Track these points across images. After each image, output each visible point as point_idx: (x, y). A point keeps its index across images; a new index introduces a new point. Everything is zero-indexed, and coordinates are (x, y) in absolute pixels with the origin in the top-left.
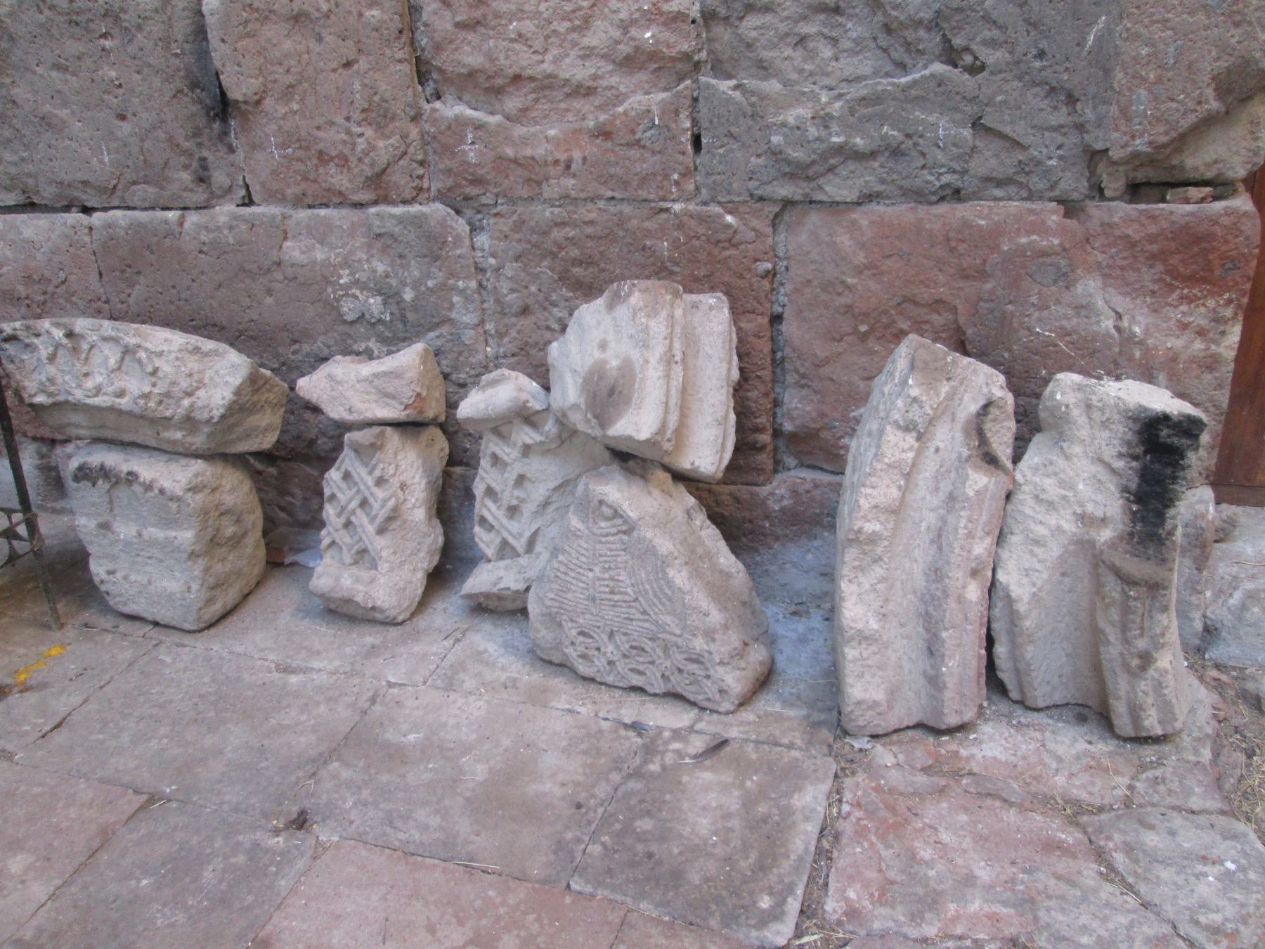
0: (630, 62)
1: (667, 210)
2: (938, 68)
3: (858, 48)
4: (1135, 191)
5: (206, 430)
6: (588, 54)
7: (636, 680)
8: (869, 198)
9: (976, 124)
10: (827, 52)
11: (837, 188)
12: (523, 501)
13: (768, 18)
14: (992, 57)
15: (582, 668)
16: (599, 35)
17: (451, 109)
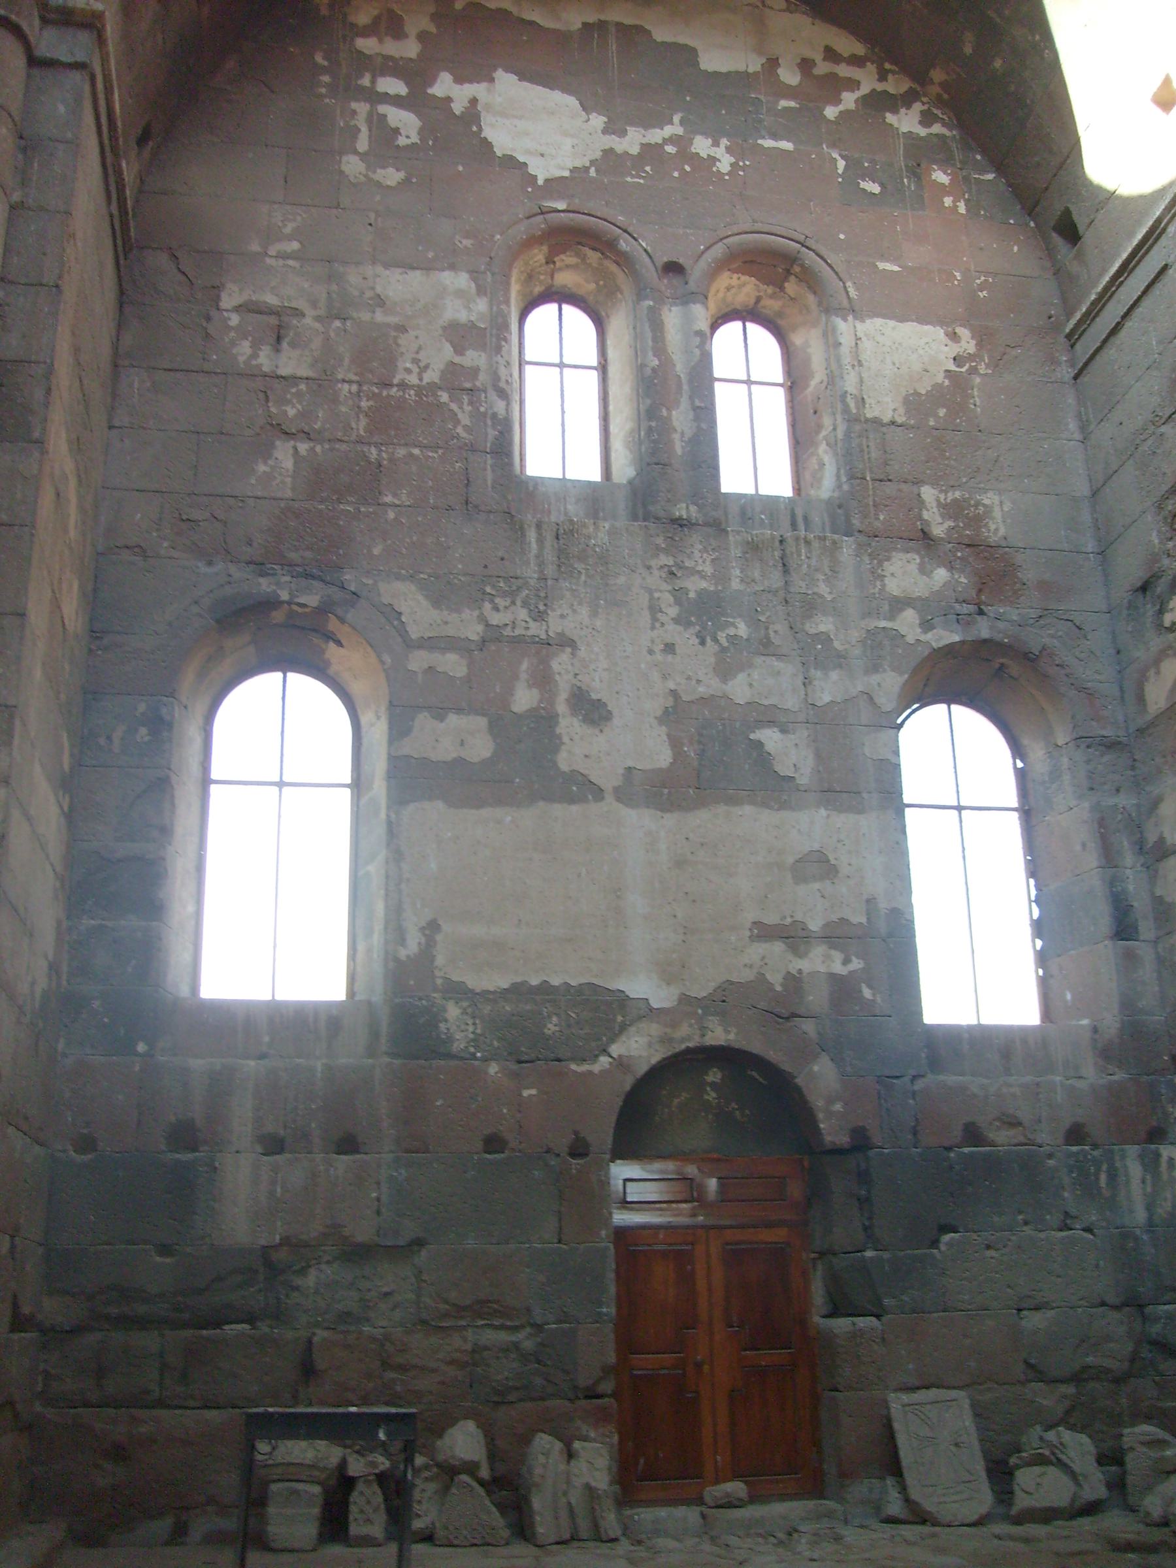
0: (452, 1362)
1: (463, 1406)
2: (536, 1365)
3: (514, 1360)
4: (587, 1397)
5: (328, 1472)
6: (438, 1360)
7: (475, 1541)
8: (521, 1400)
9: (546, 1379)
10: (505, 1361)
11: (511, 1397)
12: (422, 1498)
13: (490, 1352)
14: (549, 1363)
15: (456, 1542)
16: (441, 1355)
17: (391, 1375)
